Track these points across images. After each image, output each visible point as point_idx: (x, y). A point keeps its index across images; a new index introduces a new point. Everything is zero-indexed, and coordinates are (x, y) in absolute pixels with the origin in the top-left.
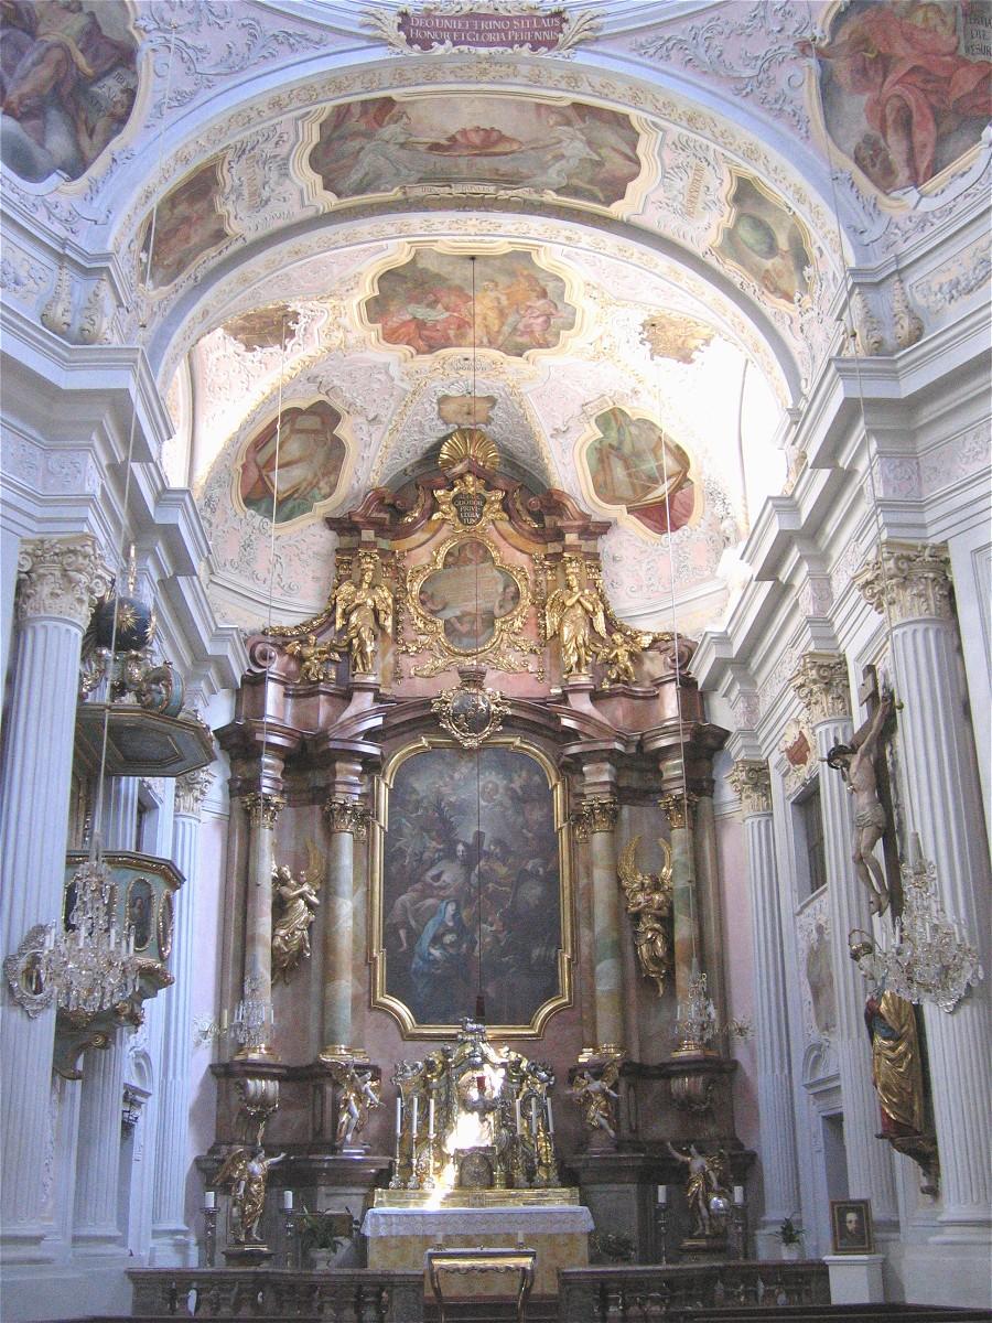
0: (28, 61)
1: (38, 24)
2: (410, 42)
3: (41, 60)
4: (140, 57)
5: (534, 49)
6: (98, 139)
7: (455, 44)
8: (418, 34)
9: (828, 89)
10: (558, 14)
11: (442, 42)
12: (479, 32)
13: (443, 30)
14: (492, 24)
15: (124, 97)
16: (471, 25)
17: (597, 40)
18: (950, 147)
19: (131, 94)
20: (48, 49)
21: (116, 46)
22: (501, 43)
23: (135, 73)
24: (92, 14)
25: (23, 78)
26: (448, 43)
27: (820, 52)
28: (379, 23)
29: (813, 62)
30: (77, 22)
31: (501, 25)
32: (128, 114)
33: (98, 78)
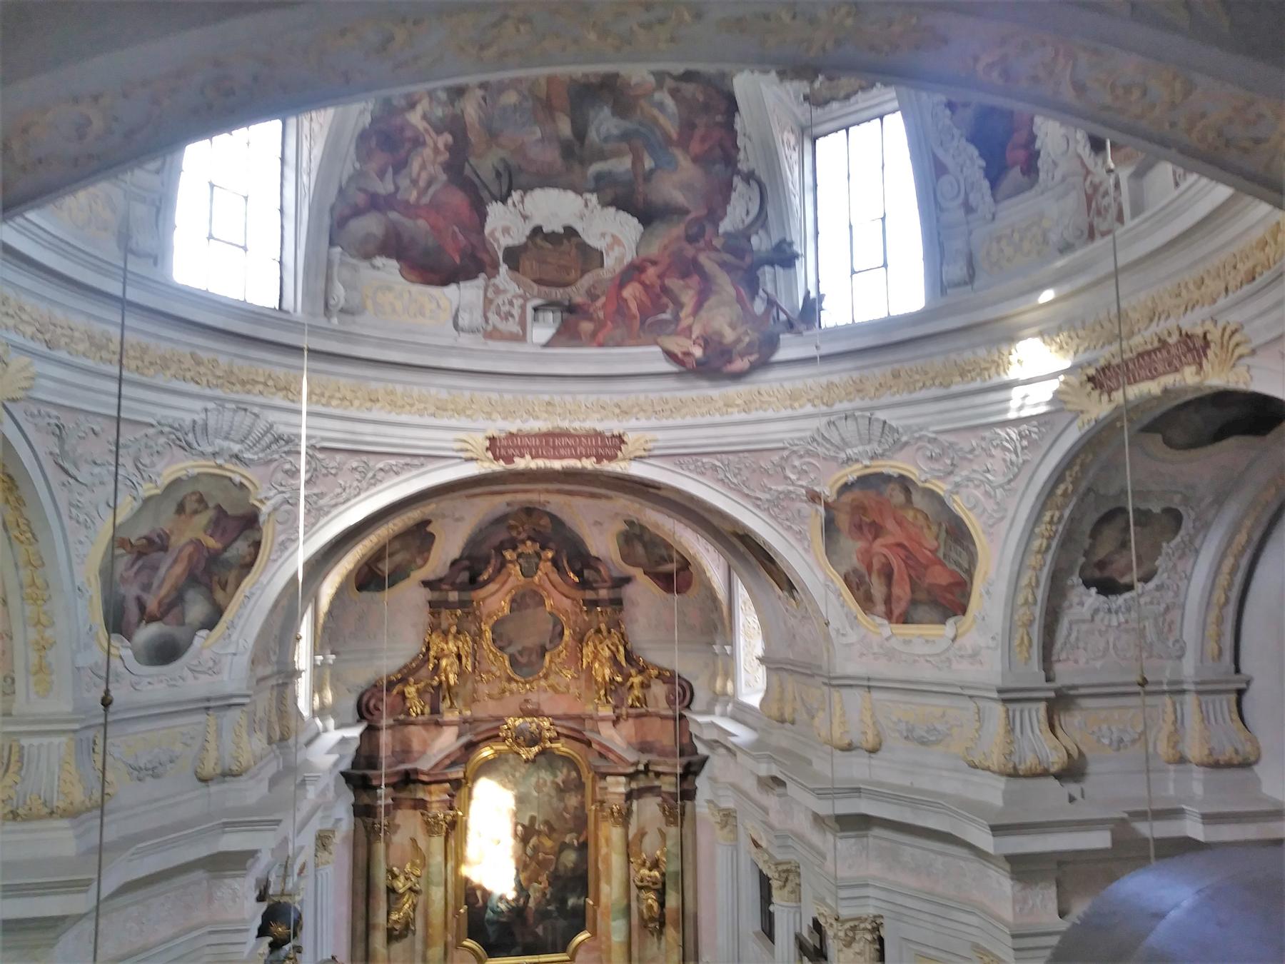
0: (163, 571)
1: (168, 537)
2: (496, 458)
3: (175, 561)
4: (262, 519)
5: (599, 461)
6: (230, 588)
7: (533, 458)
8: (503, 452)
9: (830, 527)
10: (620, 437)
11: (522, 456)
12: (554, 447)
13: (523, 447)
14: (564, 441)
15: (252, 549)
16: (547, 443)
17: (650, 457)
18: (921, 611)
19: (257, 545)
20: (181, 551)
21: (242, 517)
22: (572, 457)
23: (260, 530)
24: (219, 507)
25: (160, 586)
26: (528, 457)
27: (827, 506)
28: (469, 447)
29: (822, 509)
30: (203, 519)
31: (571, 442)
32: (251, 564)
33: (225, 549)
